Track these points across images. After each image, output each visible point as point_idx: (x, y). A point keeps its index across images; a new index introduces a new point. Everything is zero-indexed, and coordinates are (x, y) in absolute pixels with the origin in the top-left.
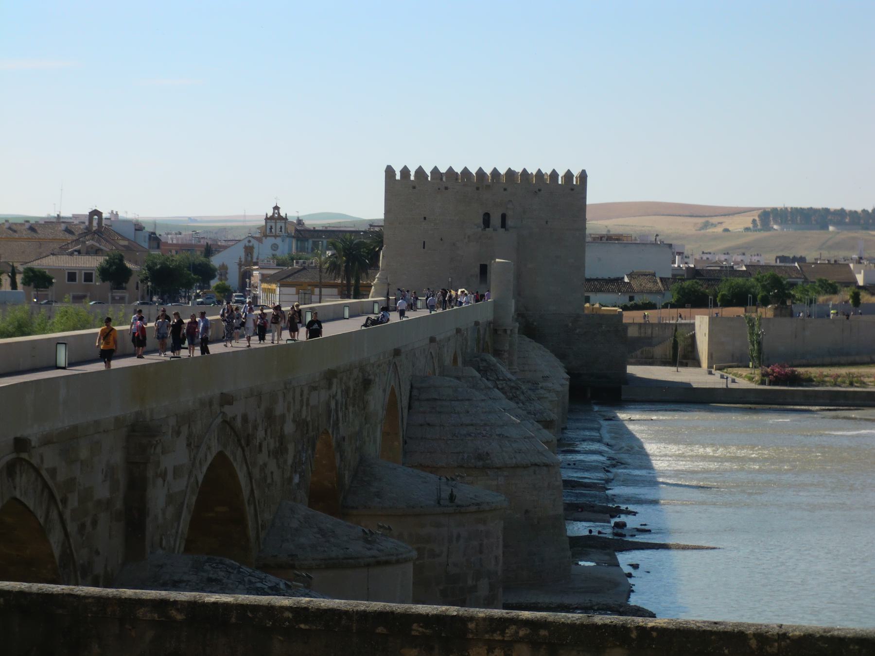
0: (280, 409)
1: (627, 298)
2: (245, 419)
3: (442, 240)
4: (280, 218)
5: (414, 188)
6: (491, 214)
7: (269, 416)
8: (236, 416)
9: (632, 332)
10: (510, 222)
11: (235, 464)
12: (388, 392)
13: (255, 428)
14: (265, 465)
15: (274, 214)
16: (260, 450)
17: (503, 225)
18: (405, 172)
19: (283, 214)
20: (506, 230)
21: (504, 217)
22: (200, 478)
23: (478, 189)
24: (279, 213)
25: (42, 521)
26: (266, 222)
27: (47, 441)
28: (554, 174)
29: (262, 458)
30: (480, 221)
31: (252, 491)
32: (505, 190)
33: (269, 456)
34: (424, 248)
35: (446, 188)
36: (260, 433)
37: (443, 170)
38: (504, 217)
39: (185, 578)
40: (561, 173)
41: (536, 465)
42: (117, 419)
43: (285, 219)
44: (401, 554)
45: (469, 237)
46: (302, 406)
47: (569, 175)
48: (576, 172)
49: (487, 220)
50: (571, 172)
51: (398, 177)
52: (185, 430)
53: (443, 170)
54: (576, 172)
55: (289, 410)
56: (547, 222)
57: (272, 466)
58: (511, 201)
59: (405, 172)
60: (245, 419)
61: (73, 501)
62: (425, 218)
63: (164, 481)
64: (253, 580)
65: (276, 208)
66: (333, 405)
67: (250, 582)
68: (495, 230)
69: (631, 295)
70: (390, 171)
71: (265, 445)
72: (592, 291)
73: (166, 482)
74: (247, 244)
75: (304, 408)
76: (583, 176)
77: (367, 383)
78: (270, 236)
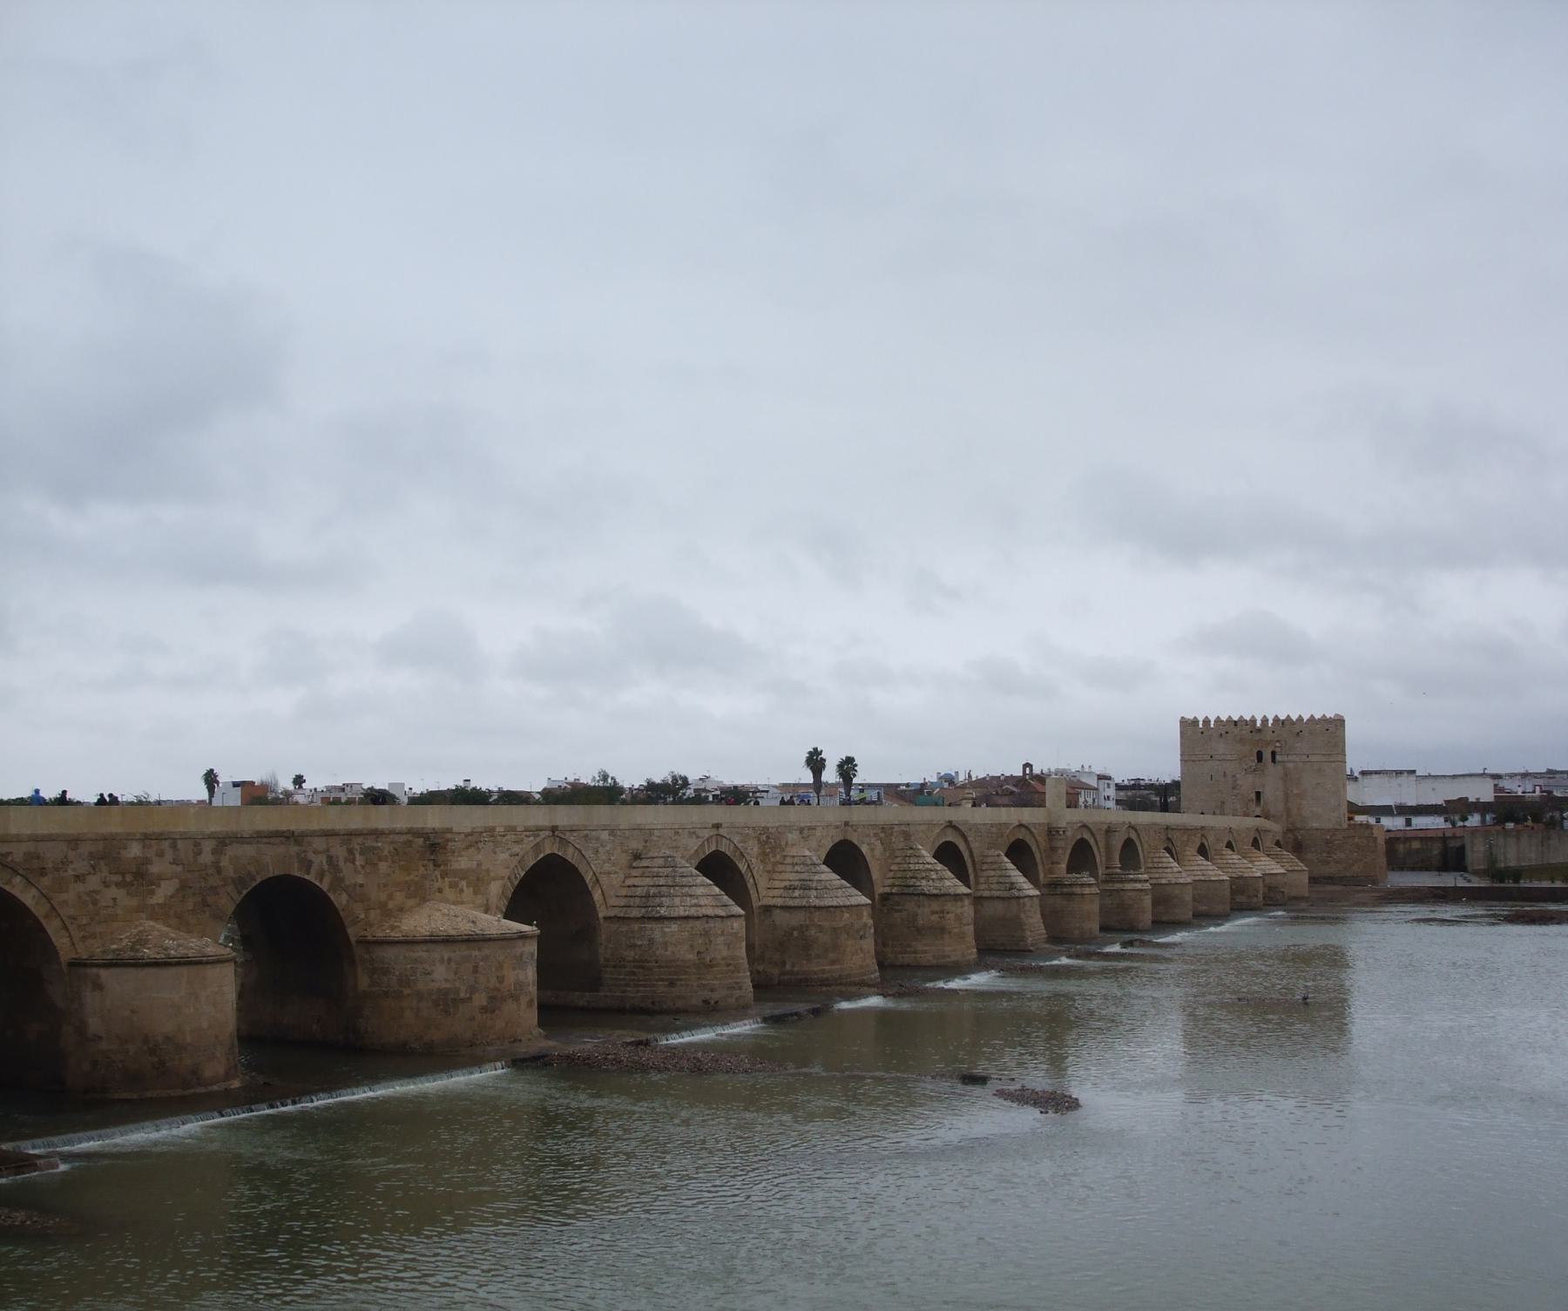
13: (65, 862)
17: (1274, 760)
30: (1255, 758)
35: (1227, 733)
37: (1224, 718)
38: (1273, 754)
41: (707, 916)
49: (1260, 756)
53: (1224, 718)
55: (161, 854)
60: (30, 856)
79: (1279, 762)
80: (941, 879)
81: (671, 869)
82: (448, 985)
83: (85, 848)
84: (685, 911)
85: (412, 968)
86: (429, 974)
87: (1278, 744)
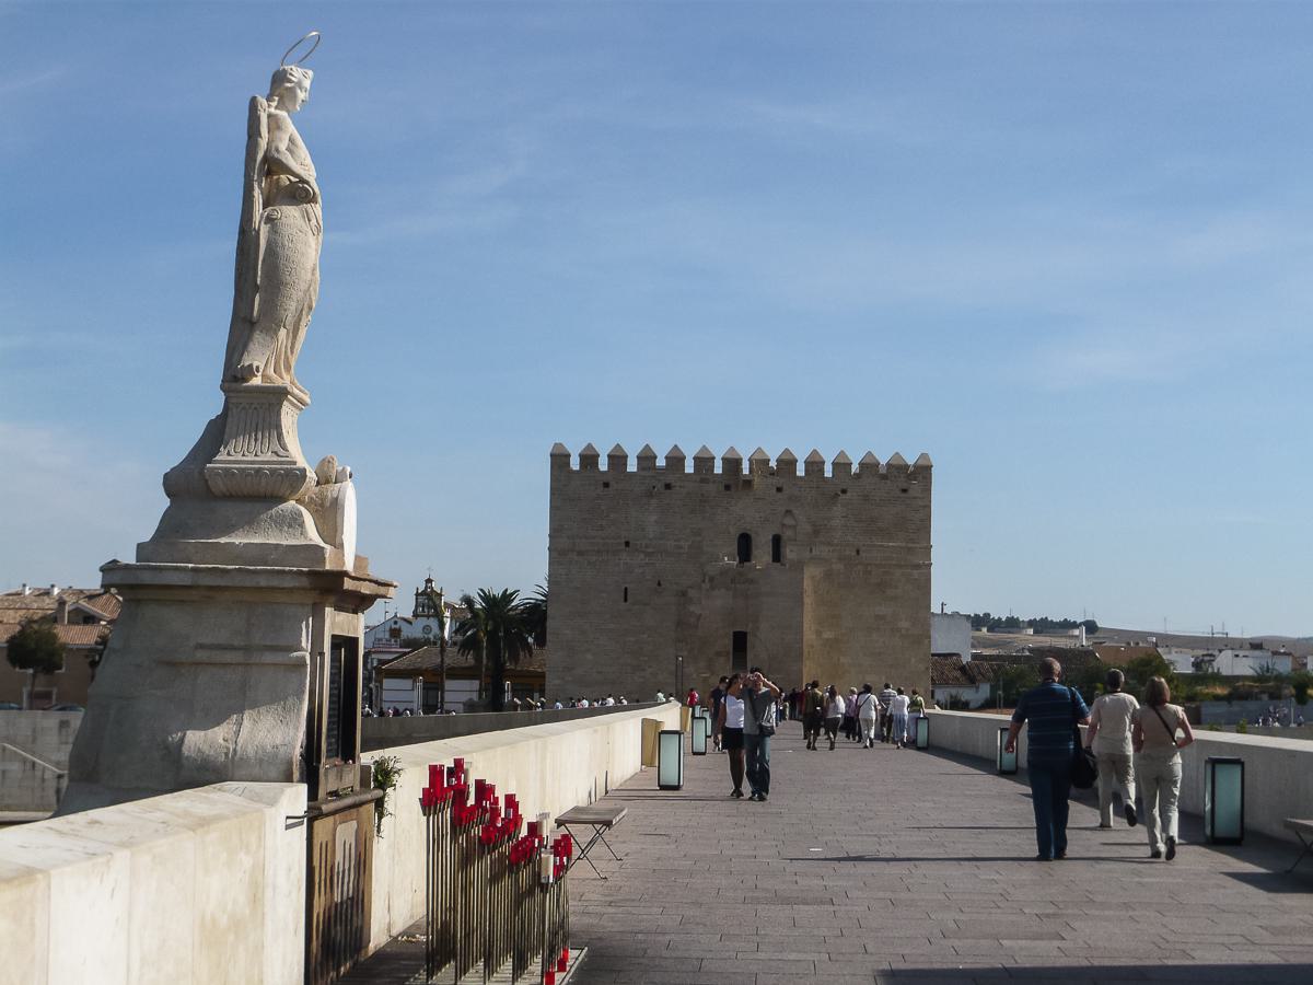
3: (659, 584)
5: (606, 485)
6: (753, 536)
10: (790, 553)
17: (777, 556)
23: (727, 487)
32: (779, 490)
34: (626, 600)
38: (777, 541)
49: (745, 546)
51: (575, 464)
56: (858, 552)
58: (787, 511)
62: (627, 544)
70: (559, 459)
74: (394, 626)
87: (789, 521)
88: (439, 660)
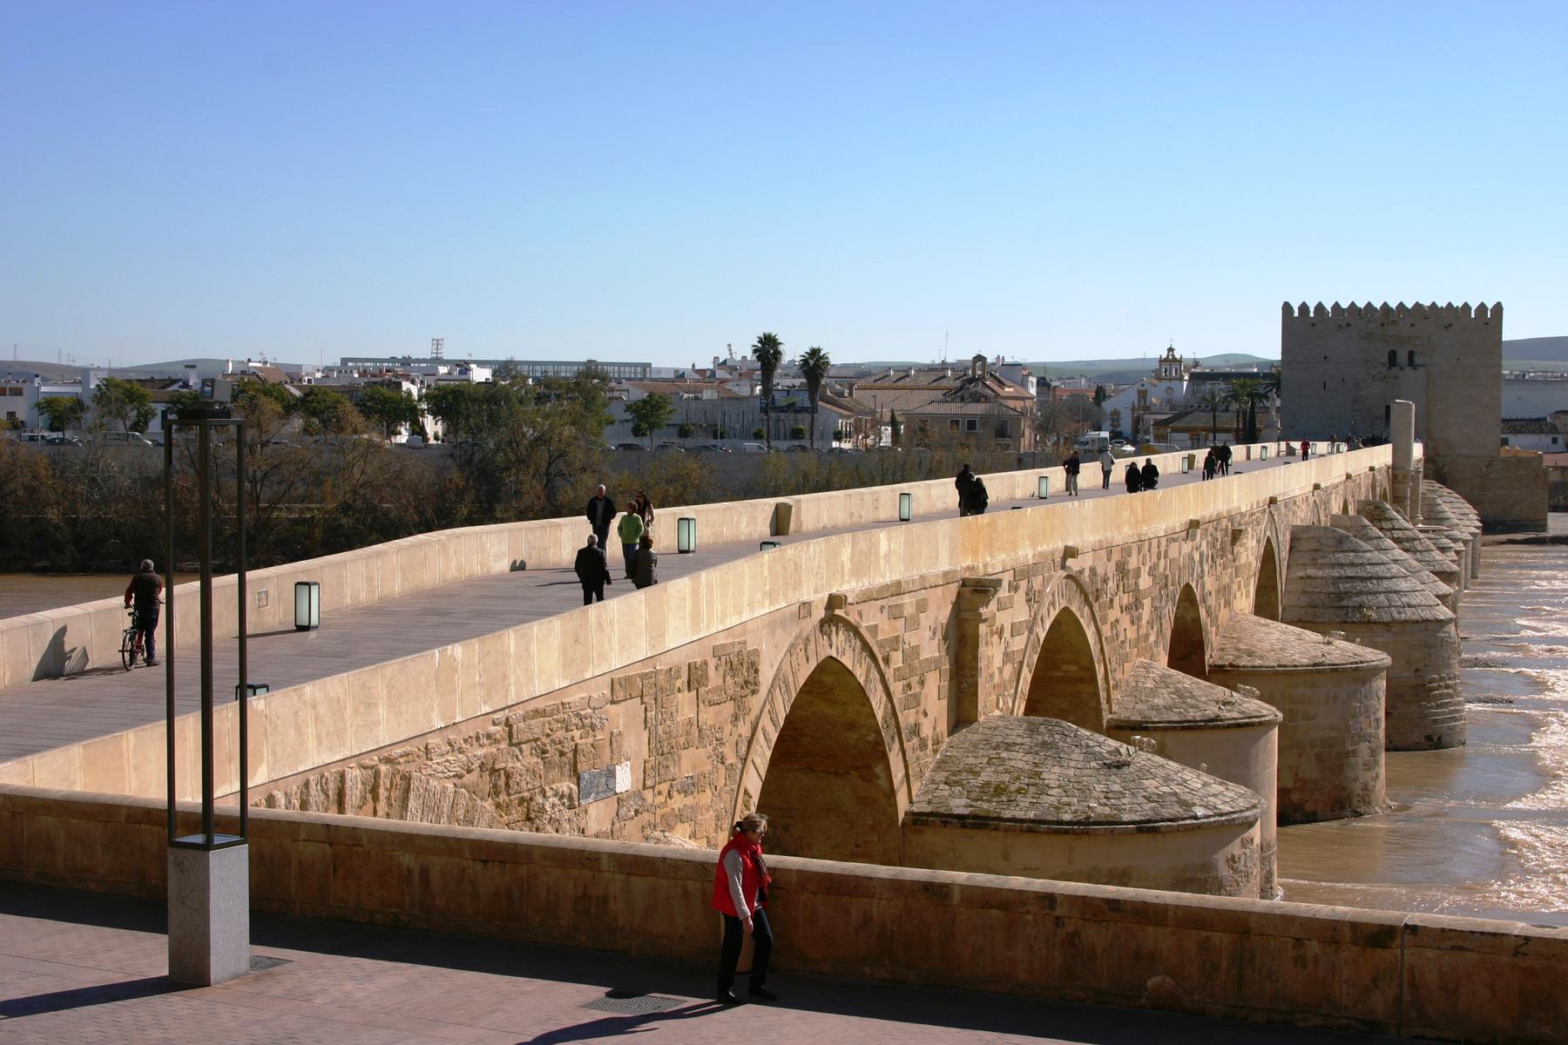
0: (1133, 562)
1: (1549, 439)
2: (1093, 570)
3: (1343, 380)
4: (1174, 359)
6: (1398, 352)
7: (1122, 569)
8: (1084, 569)
9: (1555, 477)
10: (1417, 360)
11: (1081, 620)
12: (1263, 543)
13: (1105, 581)
14: (1117, 621)
15: (1168, 356)
16: (1111, 607)
17: (1411, 362)
18: (1304, 308)
19: (1178, 357)
20: (1415, 368)
21: (1411, 354)
22: (1042, 636)
23: (1383, 325)
24: (1173, 356)
25: (861, 681)
26: (1160, 365)
27: (868, 597)
28: (1466, 306)
29: (1114, 614)
30: (1385, 359)
31: (1102, 650)
32: (1412, 325)
33: (1122, 612)
35: (1348, 325)
36: (1111, 585)
38: (1411, 354)
39: (1019, 740)
40: (1474, 306)
42: (946, 574)
43: (1180, 361)
44: (1264, 716)
45: (1373, 376)
46: (1159, 559)
47: (1482, 307)
48: (1490, 306)
49: (1392, 356)
50: (1403, 305)
51: (1296, 314)
52: (1023, 584)
54: (1490, 306)
57: (1125, 621)
59: (1304, 308)
60: (1093, 570)
61: (897, 659)
62: (1325, 357)
63: (1001, 639)
64: (1091, 743)
65: (1171, 350)
66: (1197, 557)
67: (1088, 746)
68: (1402, 369)
69: (1554, 436)
70: (1287, 308)
71: (1116, 600)
72: (1511, 433)
73: (1003, 639)
74: (1141, 388)
75: (1162, 560)
76: (1498, 308)
77: (1236, 536)
78: (1165, 379)
79: (1420, 366)
80: (1428, 551)
81: (1352, 554)
82: (1333, 734)
83: (1116, 557)
84: (1400, 613)
85: (1291, 710)
86: (1314, 718)
88: (1212, 424)
